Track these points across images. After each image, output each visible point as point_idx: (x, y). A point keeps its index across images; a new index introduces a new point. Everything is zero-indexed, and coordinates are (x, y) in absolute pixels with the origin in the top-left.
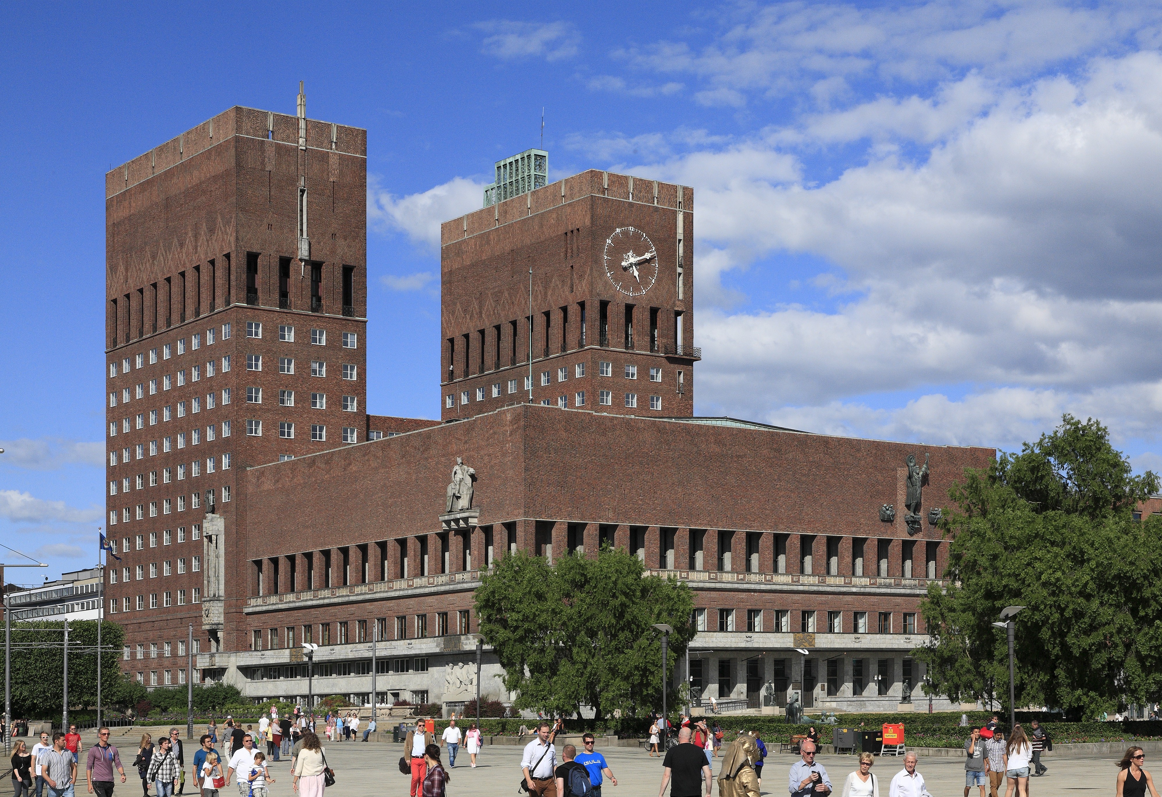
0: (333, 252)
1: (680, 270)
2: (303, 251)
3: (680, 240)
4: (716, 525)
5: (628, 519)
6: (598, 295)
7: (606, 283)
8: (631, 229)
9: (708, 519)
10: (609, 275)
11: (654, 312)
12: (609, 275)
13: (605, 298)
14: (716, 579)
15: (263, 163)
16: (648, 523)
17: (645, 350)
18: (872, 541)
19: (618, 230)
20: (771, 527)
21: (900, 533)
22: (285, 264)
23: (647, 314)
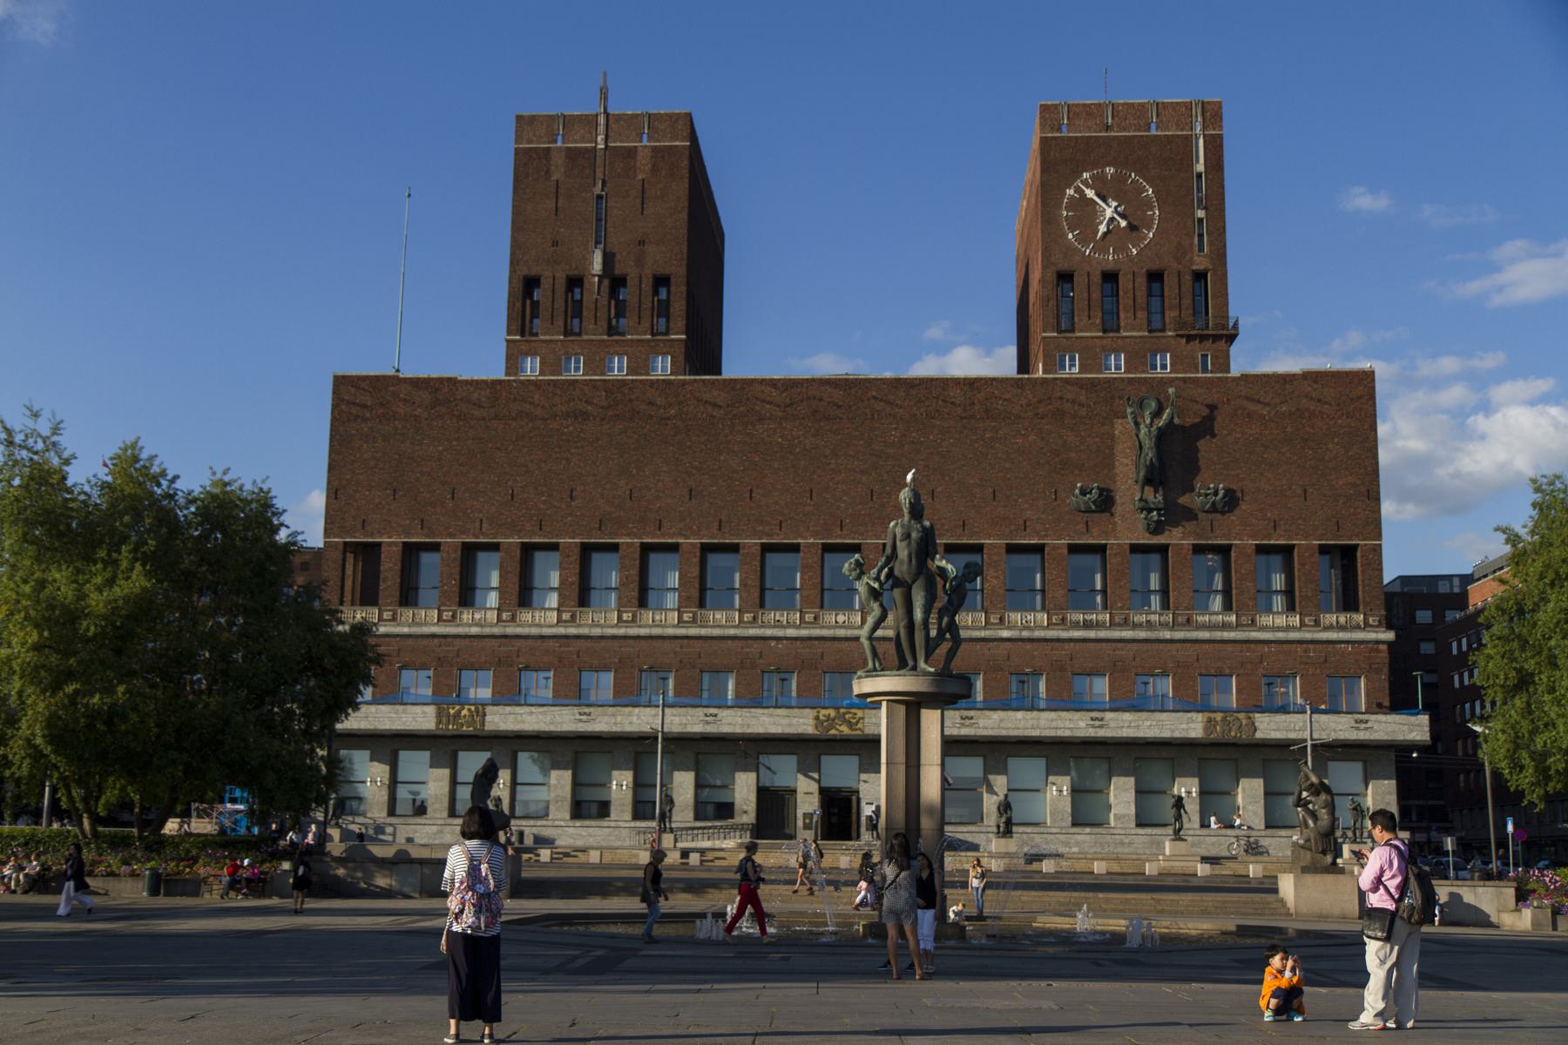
0: (639, 261)
1: (1201, 214)
2: (597, 265)
3: (1199, 175)
4: (697, 534)
5: (519, 533)
7: (1069, 250)
8: (1110, 170)
11: (1155, 277)
13: (1064, 266)
15: (547, 172)
16: (557, 536)
18: (1055, 547)
19: (1085, 175)
20: (815, 535)
21: (1127, 528)
22: (575, 282)
23: (1141, 281)
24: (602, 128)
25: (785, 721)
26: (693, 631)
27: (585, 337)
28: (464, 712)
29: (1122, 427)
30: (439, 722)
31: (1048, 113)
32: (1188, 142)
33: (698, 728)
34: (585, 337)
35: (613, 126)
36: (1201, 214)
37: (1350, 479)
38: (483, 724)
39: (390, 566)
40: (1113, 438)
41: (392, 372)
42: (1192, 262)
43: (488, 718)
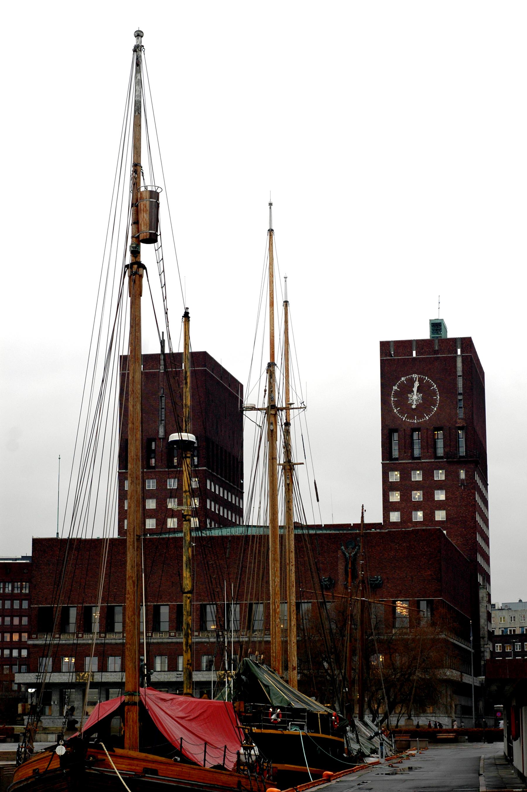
1: (460, 397)
6: (387, 425)
7: (394, 416)
9: (169, 597)
10: (395, 411)
12: (395, 411)
13: (392, 426)
14: (175, 636)
17: (429, 459)
19: (403, 379)
24: (162, 362)
25: (207, 676)
26: (174, 640)
27: (157, 470)
28: (86, 675)
29: (340, 554)
30: (76, 679)
31: (385, 346)
32: (455, 358)
33: (174, 680)
34: (157, 470)
35: (168, 361)
36: (460, 397)
37: (430, 573)
38: (93, 679)
39: (57, 615)
40: (337, 558)
41: (55, 536)
42: (456, 423)
43: (95, 677)
